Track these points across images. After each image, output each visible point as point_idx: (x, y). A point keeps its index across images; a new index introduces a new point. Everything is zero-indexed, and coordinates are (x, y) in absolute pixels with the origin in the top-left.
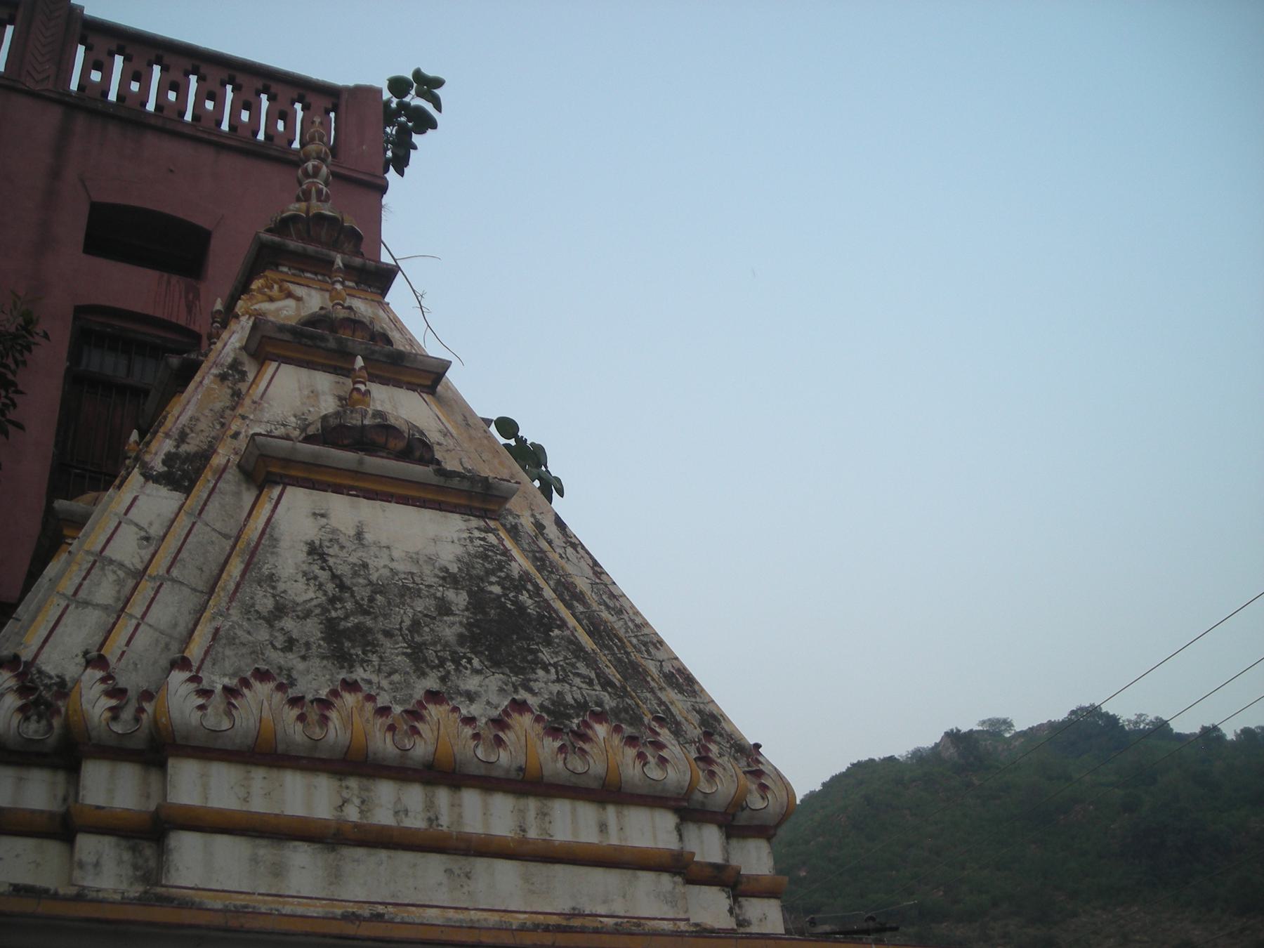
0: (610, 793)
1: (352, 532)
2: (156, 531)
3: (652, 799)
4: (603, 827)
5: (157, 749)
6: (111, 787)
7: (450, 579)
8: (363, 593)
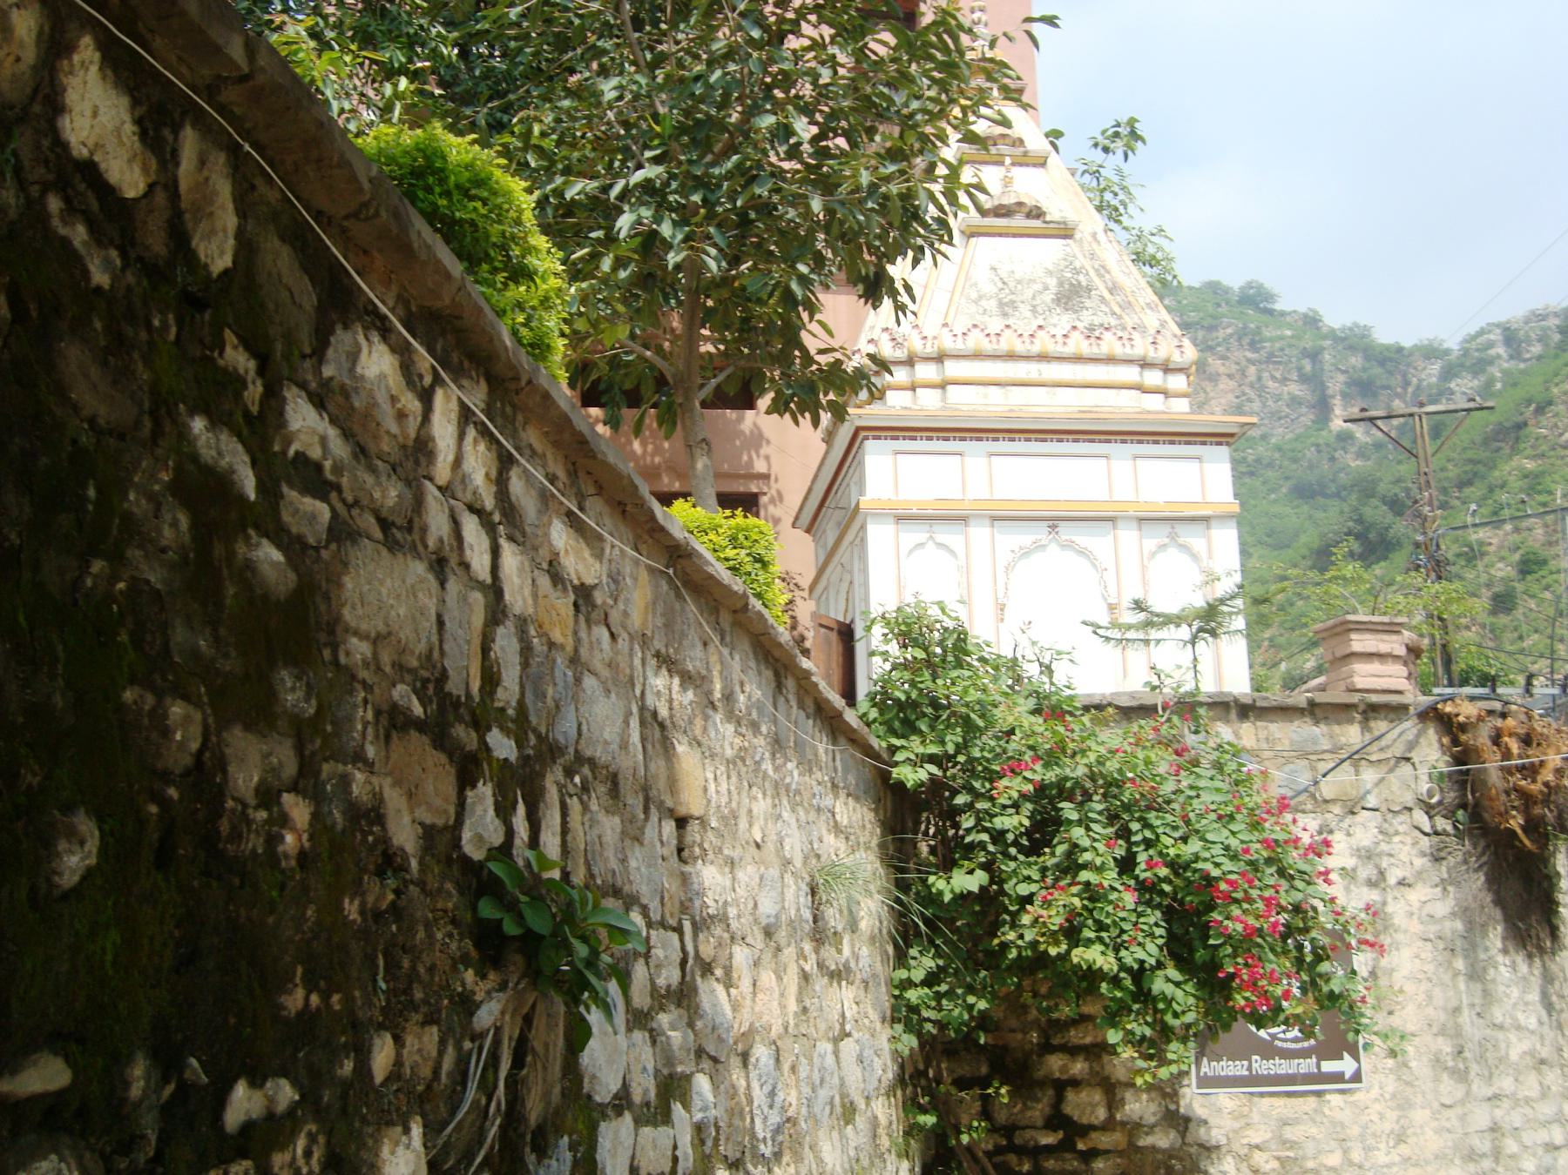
0: (1110, 360)
3: (1129, 361)
5: (940, 358)
6: (925, 372)
7: (1050, 273)
8: (1012, 284)
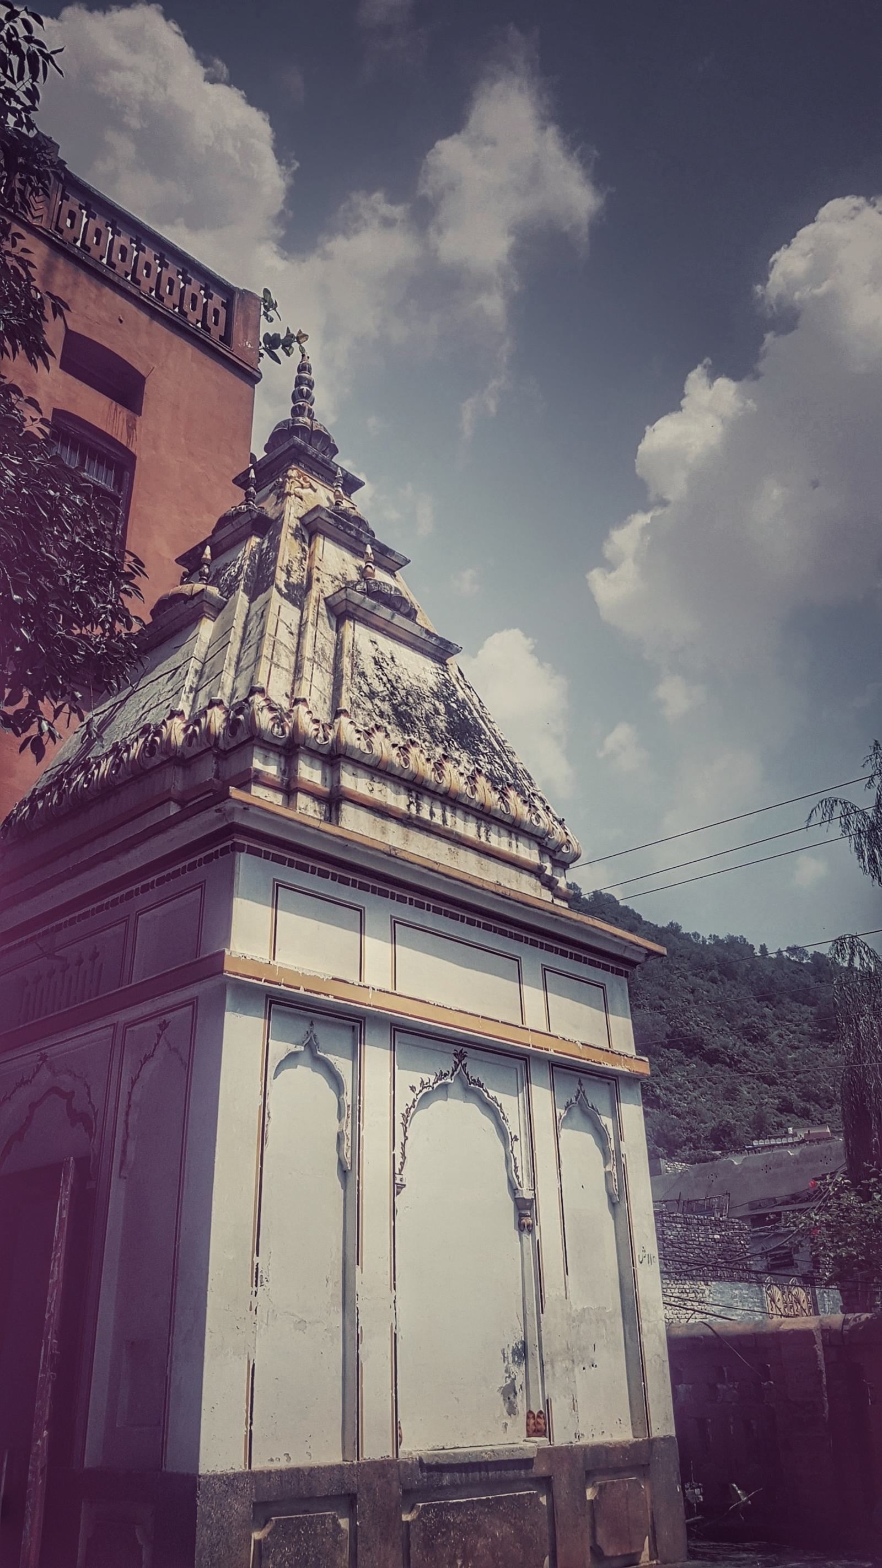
0: (514, 828)
1: (389, 656)
2: (295, 629)
4: (510, 844)
6: (310, 773)
7: (435, 695)
